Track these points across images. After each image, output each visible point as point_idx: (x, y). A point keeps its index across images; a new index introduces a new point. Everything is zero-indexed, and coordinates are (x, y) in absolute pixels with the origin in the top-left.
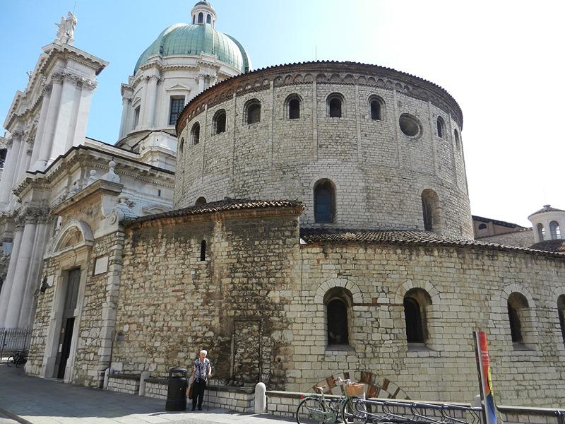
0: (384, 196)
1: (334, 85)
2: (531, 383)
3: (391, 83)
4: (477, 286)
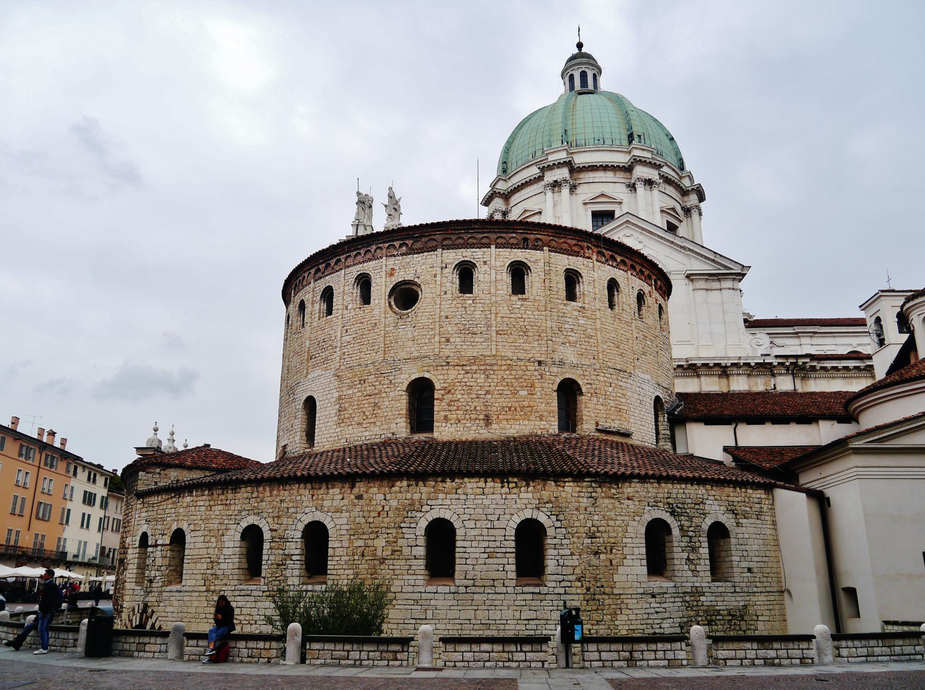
0: (355, 403)
3: (381, 248)
4: (218, 522)
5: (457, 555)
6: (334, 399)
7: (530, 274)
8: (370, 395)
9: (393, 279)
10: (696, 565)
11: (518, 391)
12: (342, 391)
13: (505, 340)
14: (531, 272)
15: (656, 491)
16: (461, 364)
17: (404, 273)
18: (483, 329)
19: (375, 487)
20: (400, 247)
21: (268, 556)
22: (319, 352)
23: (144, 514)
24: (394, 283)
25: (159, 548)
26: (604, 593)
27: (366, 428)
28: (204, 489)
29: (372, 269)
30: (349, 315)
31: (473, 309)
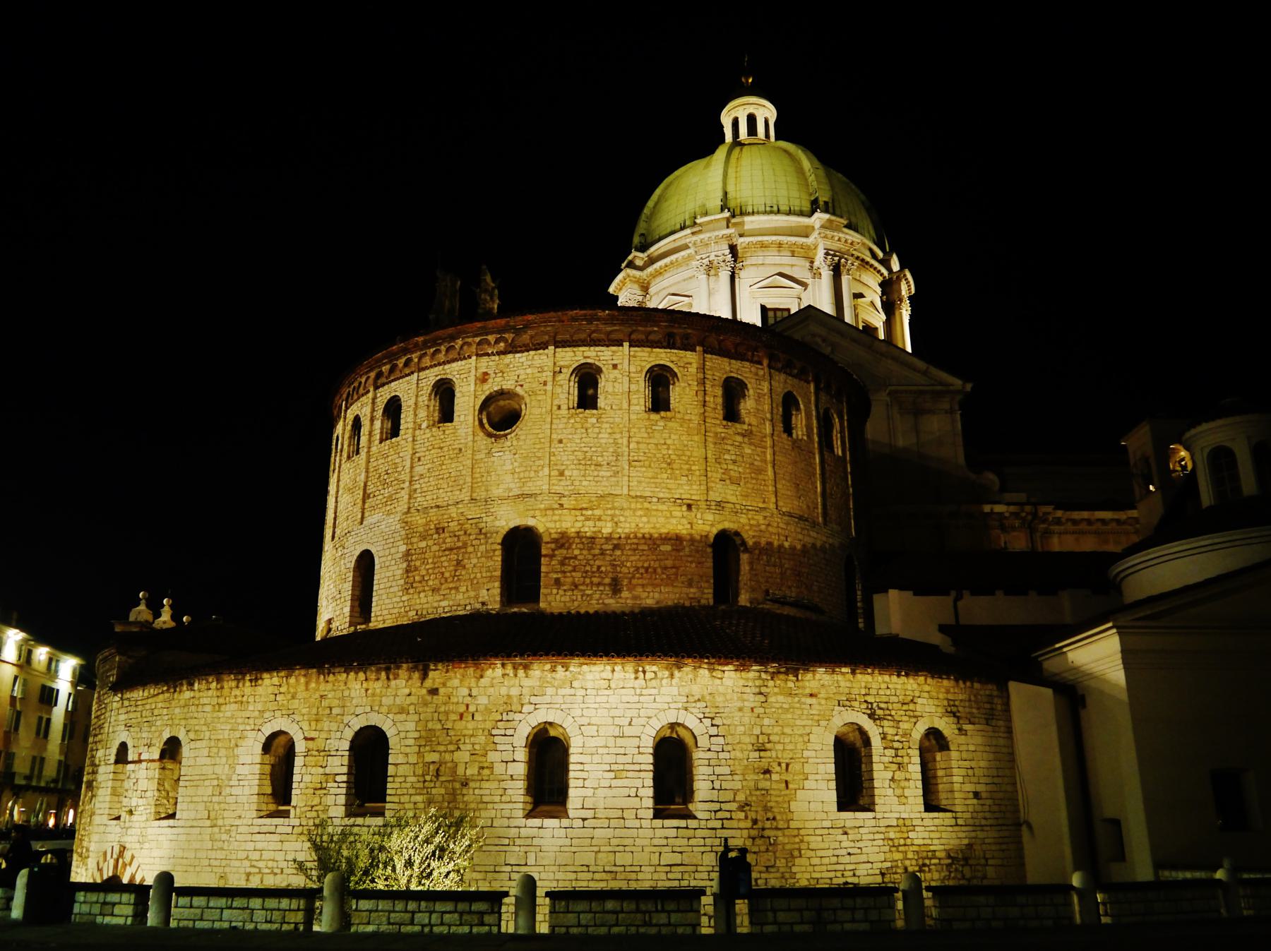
0: (430, 561)
1: (393, 384)
2: (270, 864)
4: (229, 727)
5: (571, 774)
6: (400, 555)
7: (677, 384)
8: (451, 549)
9: (486, 387)
10: (903, 788)
11: (659, 546)
12: (411, 544)
13: (641, 475)
14: (678, 380)
15: (848, 684)
16: (580, 507)
17: (501, 379)
18: (611, 458)
19: (456, 678)
20: (495, 343)
21: (303, 775)
22: (380, 488)
23: (122, 717)
24: (487, 393)
25: (144, 764)
26: (777, 829)
27: (444, 595)
28: (210, 680)
29: (456, 373)
30: (423, 437)
31: (597, 430)
